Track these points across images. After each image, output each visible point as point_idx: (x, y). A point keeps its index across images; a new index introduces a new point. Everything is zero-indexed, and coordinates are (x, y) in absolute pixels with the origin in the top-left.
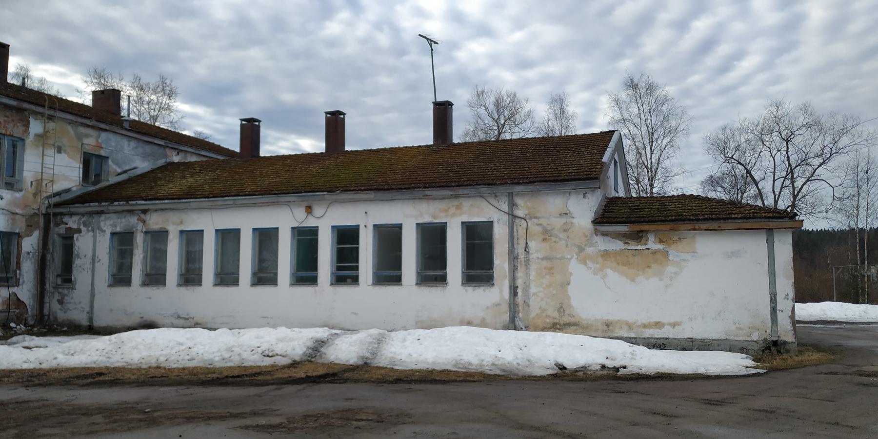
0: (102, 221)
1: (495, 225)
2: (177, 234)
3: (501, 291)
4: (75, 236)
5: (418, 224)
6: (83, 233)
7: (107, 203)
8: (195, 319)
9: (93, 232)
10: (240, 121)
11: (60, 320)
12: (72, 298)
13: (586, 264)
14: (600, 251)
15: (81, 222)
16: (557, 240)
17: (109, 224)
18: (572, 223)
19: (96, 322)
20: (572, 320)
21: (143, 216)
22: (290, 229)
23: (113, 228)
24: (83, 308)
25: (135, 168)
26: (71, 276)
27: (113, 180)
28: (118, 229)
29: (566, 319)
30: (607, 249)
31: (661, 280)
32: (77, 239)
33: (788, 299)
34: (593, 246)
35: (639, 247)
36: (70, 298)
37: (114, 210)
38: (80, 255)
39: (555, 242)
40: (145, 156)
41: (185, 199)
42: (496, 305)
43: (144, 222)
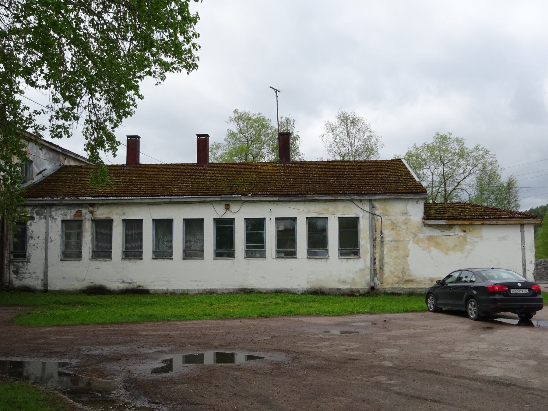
0: (53, 211)
1: (361, 219)
2: (121, 222)
3: (365, 261)
4: (29, 222)
5: (307, 218)
6: (36, 220)
7: (59, 198)
8: (137, 283)
9: (46, 220)
10: (126, 137)
11: (15, 286)
12: (27, 269)
13: (418, 244)
14: (427, 236)
15: (34, 211)
16: (401, 229)
17: (60, 213)
18: (410, 219)
19: (50, 287)
20: (410, 278)
21: (91, 209)
22: (213, 220)
23: (64, 217)
24: (37, 277)
25: (45, 170)
26: (26, 252)
27: (37, 179)
28: (68, 218)
29: (407, 278)
30: (431, 235)
31: (463, 253)
32: (31, 224)
33: (532, 264)
34: (423, 233)
35: (450, 234)
36: (25, 269)
37: (64, 203)
38: (34, 237)
39: (399, 230)
40: (50, 160)
41: (128, 197)
42: (362, 270)
43: (92, 212)
